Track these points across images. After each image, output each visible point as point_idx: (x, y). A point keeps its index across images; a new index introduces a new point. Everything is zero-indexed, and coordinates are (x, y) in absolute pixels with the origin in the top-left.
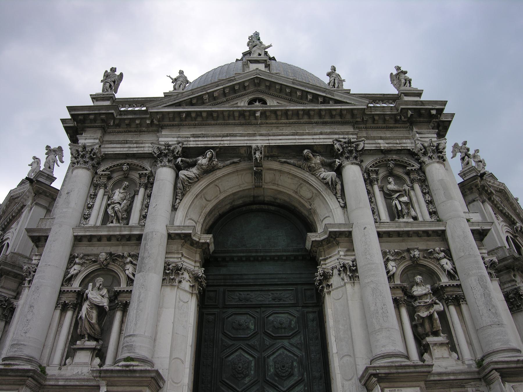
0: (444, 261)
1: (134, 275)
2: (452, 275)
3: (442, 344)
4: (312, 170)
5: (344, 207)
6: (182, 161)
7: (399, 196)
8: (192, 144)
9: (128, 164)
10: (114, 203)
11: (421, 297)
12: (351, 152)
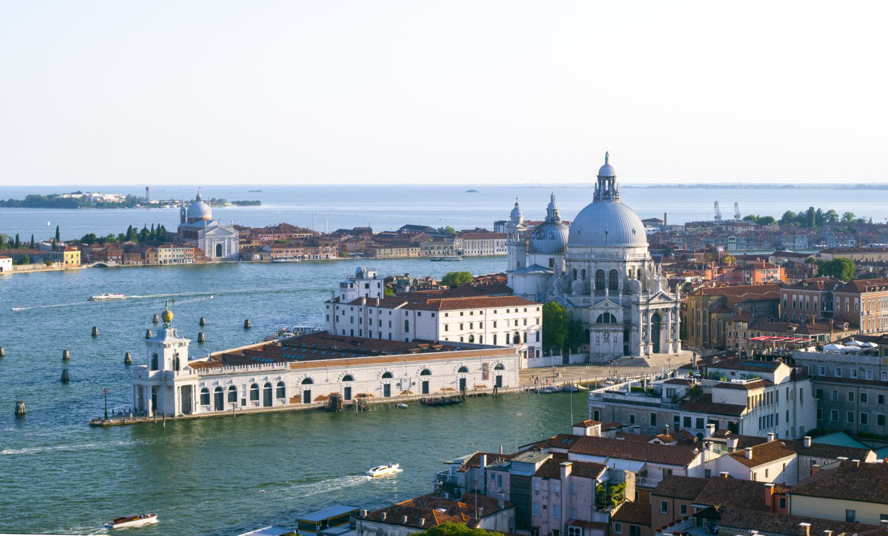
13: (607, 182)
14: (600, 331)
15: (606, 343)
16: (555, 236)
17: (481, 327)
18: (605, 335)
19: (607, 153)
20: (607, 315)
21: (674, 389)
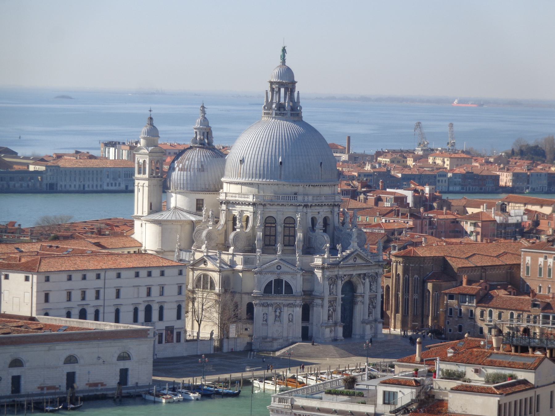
0: (375, 301)
2: (375, 303)
4: (360, 278)
13: (282, 90)
14: (268, 305)
15: (277, 323)
16: (205, 167)
17: (97, 298)
18: (275, 311)
19: (284, 50)
20: (279, 282)
21: (394, 392)
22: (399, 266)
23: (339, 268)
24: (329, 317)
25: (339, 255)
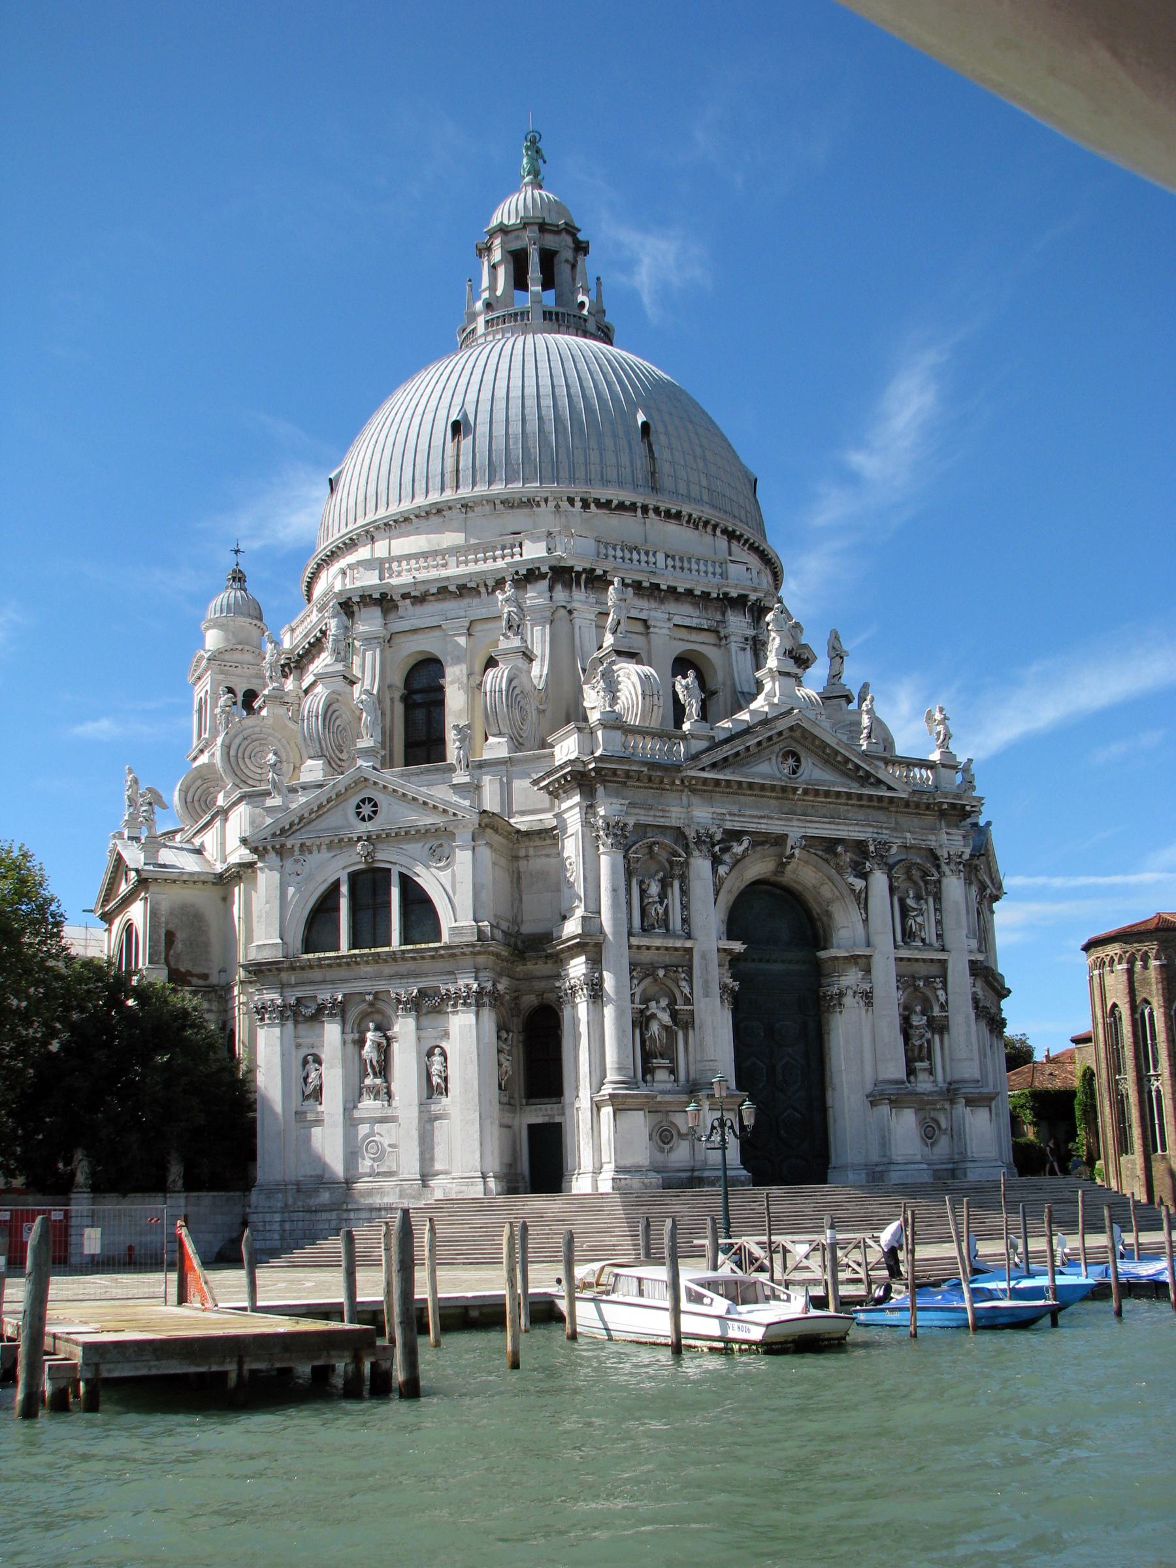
0: (940, 993)
1: (691, 994)
2: (944, 1007)
3: (925, 1070)
4: (839, 870)
5: (866, 921)
6: (720, 849)
7: (916, 916)
8: (728, 825)
9: (658, 843)
10: (656, 902)
11: (917, 1027)
12: (882, 856)
15: (369, 1105)
18: (361, 1043)
22: (1109, 980)
23: (693, 791)
24: (647, 1056)
25: (686, 726)
